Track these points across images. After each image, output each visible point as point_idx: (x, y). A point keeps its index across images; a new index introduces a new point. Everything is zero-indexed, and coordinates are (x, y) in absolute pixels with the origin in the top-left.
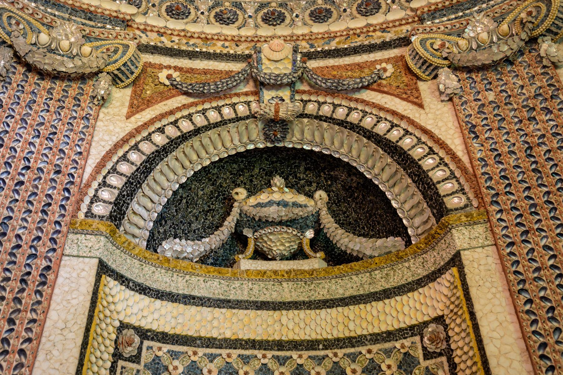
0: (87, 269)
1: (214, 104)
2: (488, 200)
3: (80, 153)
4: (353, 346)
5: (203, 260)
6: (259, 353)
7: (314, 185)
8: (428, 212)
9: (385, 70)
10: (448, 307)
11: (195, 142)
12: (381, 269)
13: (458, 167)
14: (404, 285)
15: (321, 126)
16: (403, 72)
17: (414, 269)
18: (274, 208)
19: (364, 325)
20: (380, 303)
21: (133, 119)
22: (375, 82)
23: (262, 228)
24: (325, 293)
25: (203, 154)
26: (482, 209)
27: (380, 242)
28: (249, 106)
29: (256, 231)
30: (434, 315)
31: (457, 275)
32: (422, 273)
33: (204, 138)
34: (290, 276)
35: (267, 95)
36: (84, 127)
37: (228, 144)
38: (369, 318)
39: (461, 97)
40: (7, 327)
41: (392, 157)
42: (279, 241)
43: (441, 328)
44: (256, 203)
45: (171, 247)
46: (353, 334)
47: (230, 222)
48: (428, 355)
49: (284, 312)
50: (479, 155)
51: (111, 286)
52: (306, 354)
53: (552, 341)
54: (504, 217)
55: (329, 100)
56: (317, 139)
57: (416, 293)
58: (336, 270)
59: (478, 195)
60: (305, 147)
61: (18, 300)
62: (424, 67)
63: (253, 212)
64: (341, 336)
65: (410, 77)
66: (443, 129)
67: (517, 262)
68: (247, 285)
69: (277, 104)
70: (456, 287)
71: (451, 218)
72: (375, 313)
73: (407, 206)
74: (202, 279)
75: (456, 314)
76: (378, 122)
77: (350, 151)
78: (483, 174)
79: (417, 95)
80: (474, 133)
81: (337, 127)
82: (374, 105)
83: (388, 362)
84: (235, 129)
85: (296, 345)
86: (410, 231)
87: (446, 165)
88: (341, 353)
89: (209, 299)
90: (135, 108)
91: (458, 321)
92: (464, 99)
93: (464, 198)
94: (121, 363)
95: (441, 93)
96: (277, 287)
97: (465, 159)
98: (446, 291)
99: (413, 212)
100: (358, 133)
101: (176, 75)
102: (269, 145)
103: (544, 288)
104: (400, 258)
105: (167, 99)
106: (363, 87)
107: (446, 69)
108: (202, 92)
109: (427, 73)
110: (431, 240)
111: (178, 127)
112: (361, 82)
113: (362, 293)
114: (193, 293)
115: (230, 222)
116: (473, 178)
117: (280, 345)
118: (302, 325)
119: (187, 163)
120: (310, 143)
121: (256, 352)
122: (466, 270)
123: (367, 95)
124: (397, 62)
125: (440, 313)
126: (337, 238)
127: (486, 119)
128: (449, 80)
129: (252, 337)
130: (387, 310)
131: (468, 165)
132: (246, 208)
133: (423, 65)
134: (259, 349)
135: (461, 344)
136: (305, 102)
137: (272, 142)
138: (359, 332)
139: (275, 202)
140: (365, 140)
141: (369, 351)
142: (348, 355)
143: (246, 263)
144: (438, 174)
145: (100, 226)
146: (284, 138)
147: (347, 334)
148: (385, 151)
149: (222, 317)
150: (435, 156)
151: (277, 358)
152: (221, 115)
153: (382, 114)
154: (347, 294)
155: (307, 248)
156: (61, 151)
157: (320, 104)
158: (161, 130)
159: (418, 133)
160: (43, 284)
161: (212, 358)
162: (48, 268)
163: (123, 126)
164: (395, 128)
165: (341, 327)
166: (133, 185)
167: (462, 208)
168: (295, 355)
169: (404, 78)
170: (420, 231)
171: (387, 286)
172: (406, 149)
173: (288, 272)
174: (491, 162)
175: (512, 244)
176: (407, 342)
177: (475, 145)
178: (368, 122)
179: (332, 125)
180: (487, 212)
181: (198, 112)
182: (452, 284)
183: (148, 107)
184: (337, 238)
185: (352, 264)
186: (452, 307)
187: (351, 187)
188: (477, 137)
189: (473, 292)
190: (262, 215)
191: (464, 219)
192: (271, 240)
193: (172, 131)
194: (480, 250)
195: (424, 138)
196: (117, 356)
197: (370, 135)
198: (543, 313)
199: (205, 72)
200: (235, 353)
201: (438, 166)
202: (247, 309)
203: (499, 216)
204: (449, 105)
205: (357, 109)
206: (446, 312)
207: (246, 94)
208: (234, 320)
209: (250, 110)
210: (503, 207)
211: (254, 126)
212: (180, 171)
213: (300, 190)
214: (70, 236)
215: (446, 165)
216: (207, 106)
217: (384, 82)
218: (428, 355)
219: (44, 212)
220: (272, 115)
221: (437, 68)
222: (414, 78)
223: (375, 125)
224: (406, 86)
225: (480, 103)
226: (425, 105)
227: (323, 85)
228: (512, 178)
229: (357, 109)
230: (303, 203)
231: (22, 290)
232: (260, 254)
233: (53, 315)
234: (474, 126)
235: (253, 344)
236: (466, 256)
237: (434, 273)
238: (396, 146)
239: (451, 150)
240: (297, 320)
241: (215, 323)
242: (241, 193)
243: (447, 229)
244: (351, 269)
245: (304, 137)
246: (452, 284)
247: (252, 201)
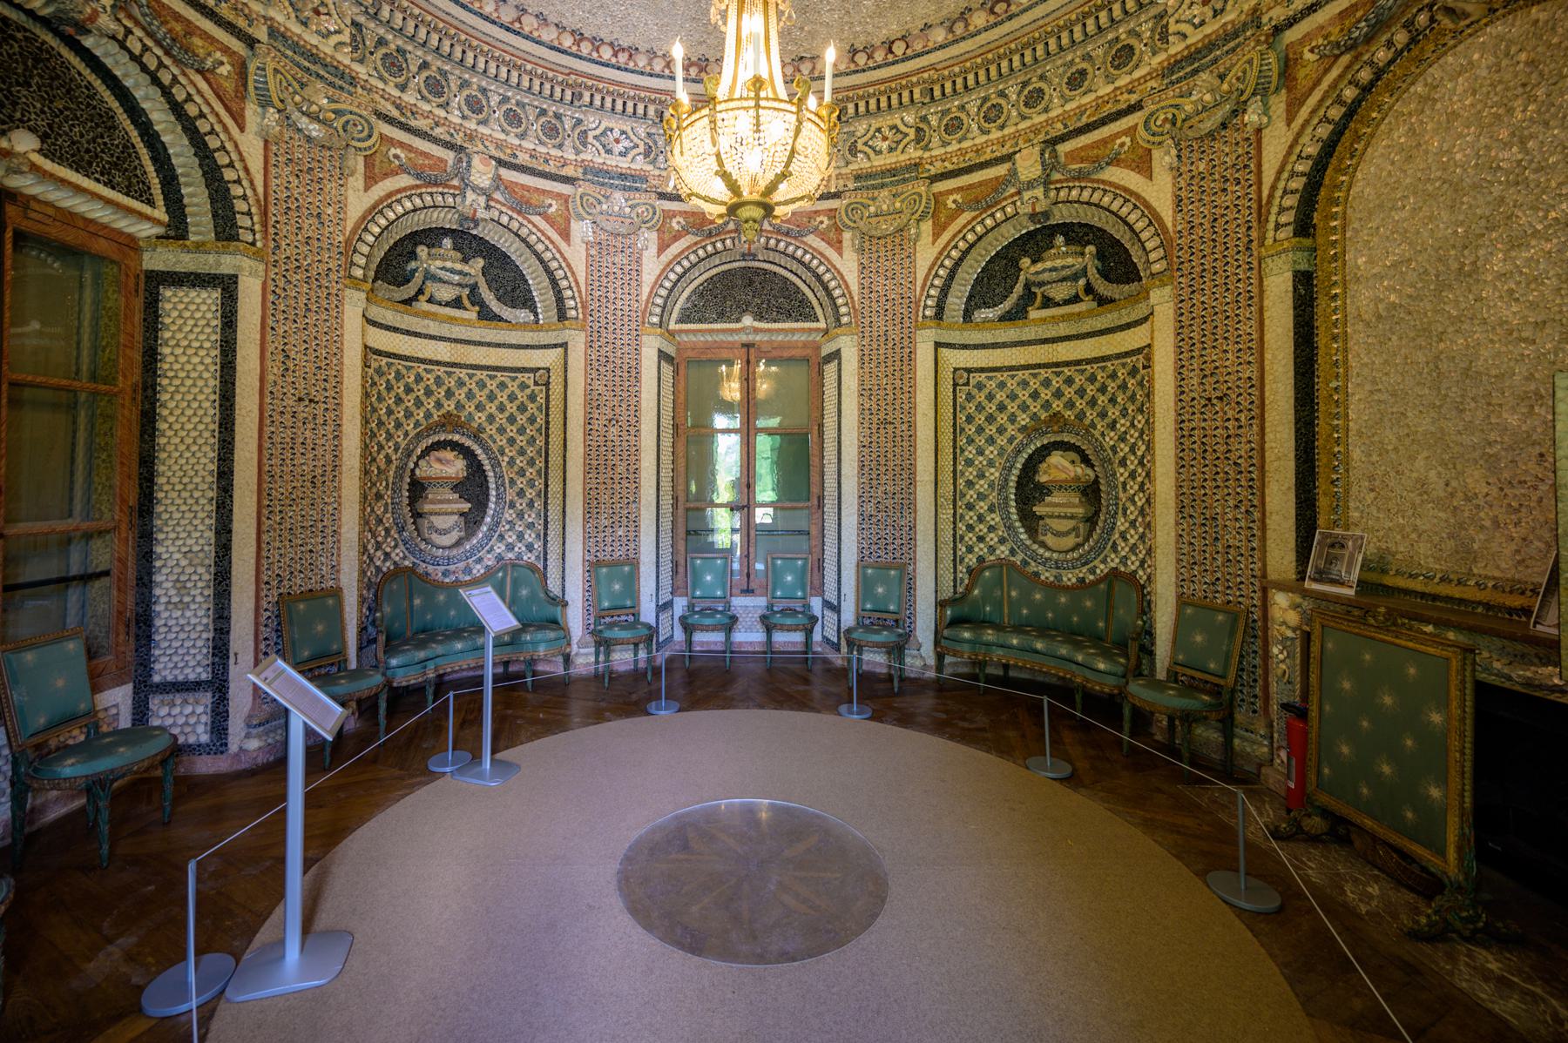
5: (1002, 319)
47: (1019, 289)
68: (1034, 329)
90: (936, 235)
101: (958, 197)
115: (1019, 289)
117: (1057, 365)
166: (945, 291)
199: (981, 184)
232: (1048, 302)
235: (1039, 366)
242: (1025, 262)
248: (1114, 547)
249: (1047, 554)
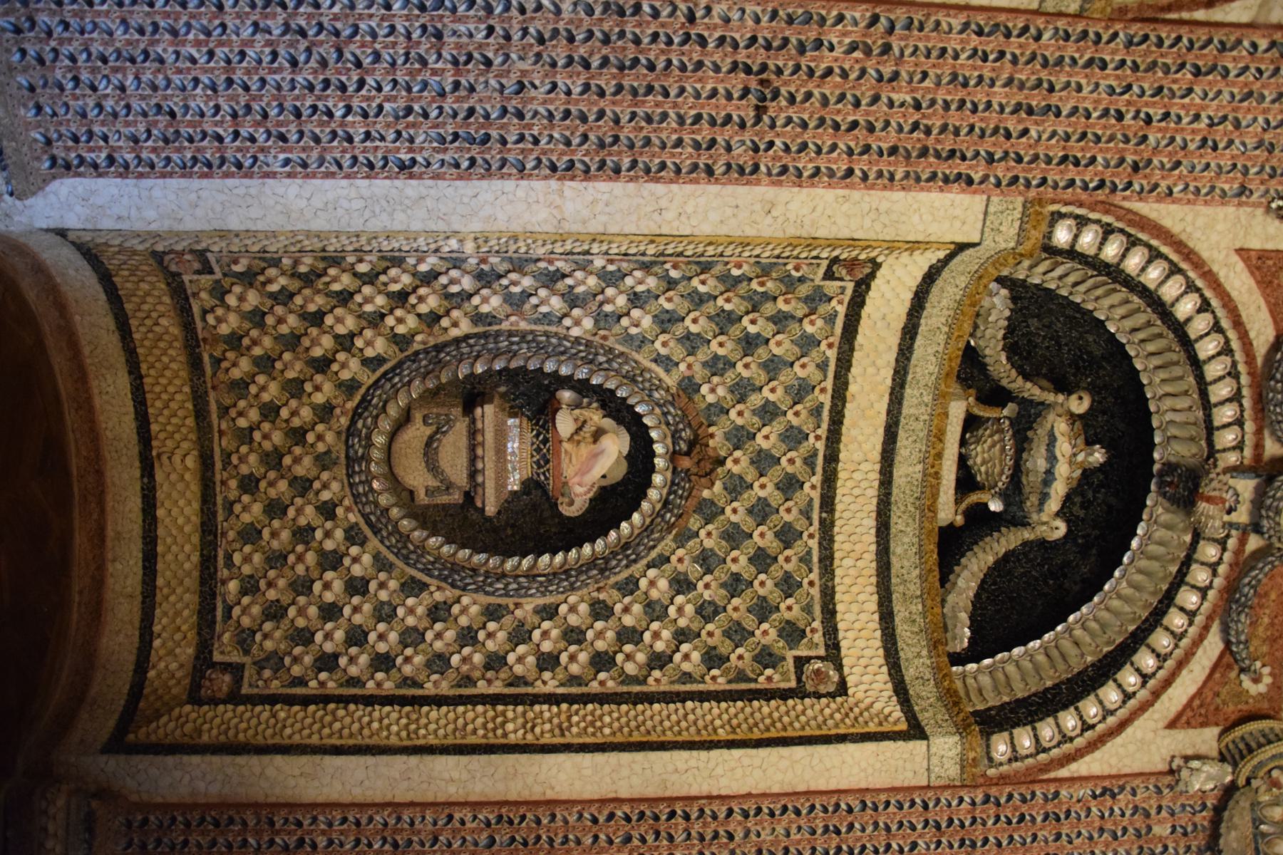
0: (966, 228)
1: (1245, 392)
2: (993, 791)
3: (1171, 193)
4: (820, 561)
6: (823, 431)
7: (1082, 513)
8: (993, 701)
9: (1256, 681)
10: (856, 705)
11: (1178, 355)
12: (924, 614)
13: (1052, 761)
14: (895, 643)
15: (1173, 560)
16: (1244, 707)
17: (917, 662)
18: (1042, 464)
19: (847, 581)
20: (874, 607)
21: (1236, 258)
22: (1236, 661)
23: (1014, 435)
24: (900, 527)
25: (1156, 361)
26: (981, 780)
27: (964, 616)
28: (1234, 448)
29: (1011, 424)
30: (851, 681)
31: (896, 728)
32: (909, 674)
33: (1183, 370)
34: (931, 477)
35: (1246, 487)
36: (1223, 190)
37: (1168, 403)
38: (855, 589)
39: (1171, 787)
40: (885, 146)
41: (1093, 665)
42: (990, 456)
43: (832, 689)
44: (1057, 434)
45: (999, 304)
46: (836, 563)
48: (800, 662)
49: (878, 467)
50: (1064, 793)
52: (816, 495)
53: (802, 822)
54: (964, 805)
55: (1218, 582)
56: (1152, 548)
57: (882, 661)
58: (932, 547)
59: (1003, 780)
60: (1142, 524)
61: (924, 152)
62: (1242, 746)
63: (1042, 432)
64: (836, 546)
65: (1233, 717)
66: (1121, 750)
67: (901, 807)
69: (1223, 501)
70: (880, 724)
71: (977, 740)
72: (862, 597)
73: (1011, 669)
74: (941, 349)
75: (847, 715)
76: (1158, 656)
77: (1119, 597)
78: (1033, 794)
79: (1193, 722)
80: (1102, 794)
81: (1165, 587)
82: (1189, 655)
83: (796, 608)
84: (1192, 420)
85: (830, 480)
86: (972, 667)
87: (1058, 745)
88: (814, 544)
89: (908, 359)
91: (837, 716)
92: (1166, 791)
93: (1004, 759)
95: (1187, 759)
96: (916, 456)
97: (1064, 773)
98: (877, 706)
99: (1000, 676)
100: (1147, 619)
102: (1156, 467)
103: (863, 830)
104: (935, 645)
105: (1271, 312)
106: (1228, 644)
107: (1229, 778)
108: (1273, 378)
109: (1231, 746)
110: (951, 699)
111: (1207, 334)
112: (1239, 642)
113: (893, 581)
114: (919, 337)
116: (1030, 778)
118: (856, 492)
119: (1141, 335)
120: (1148, 536)
121: (825, 426)
122: (901, 743)
123: (1213, 646)
124: (1270, 700)
125: (850, 692)
126: (981, 555)
127: (1123, 815)
128: (1205, 779)
129: (846, 421)
130: (864, 617)
131: (1052, 775)
132: (1051, 417)
133: (1247, 745)
134: (829, 430)
135: (810, 713)
136: (1223, 544)
137: (1161, 474)
138: (838, 572)
139: (1053, 466)
140: (1131, 628)
141: (811, 584)
142: (809, 553)
143: (957, 411)
144: (1047, 730)
145: (1033, 241)
146: (1164, 495)
147: (837, 555)
148: (1105, 656)
149: (879, 378)
150: (1078, 731)
151: (815, 454)
152: (1222, 403)
153: (1170, 663)
154: (894, 560)
155: (974, 498)
156: (1178, 164)
157: (1213, 567)
158: (1205, 307)
159: (1122, 713)
160: (946, 180)
161: (822, 367)
162: (970, 181)
163: (1223, 245)
164: (1139, 680)
165: (847, 547)
167: (988, 753)
168: (817, 479)
169: (1231, 708)
170: (970, 681)
171: (897, 620)
172: (1101, 692)
173: (937, 475)
174: (1050, 807)
175: (926, 807)
176: (818, 637)
177: (1083, 792)
178: (1162, 640)
179: (1170, 579)
180: (975, 787)
181: (1234, 364)
182: (886, 717)
183: (1258, 282)
184: (981, 555)
185: (937, 573)
186: (856, 710)
187: (1065, 576)
188: (1094, 796)
189: (870, 747)
190: (1034, 445)
191: (972, 755)
192: (993, 446)
193: (1200, 324)
194: (925, 764)
195: (1111, 720)
197: (1138, 639)
198: (835, 821)
200: (826, 399)
201: (1060, 731)
202: (889, 412)
203: (967, 799)
204: (1163, 767)
205: (1190, 624)
206: (851, 700)
207: (1259, 446)
208: (873, 397)
209: (1224, 450)
210: (979, 809)
211: (1194, 450)
212: (1128, 324)
213: (1068, 498)
214: (1020, 199)
215: (1058, 745)
216: (1244, 380)
217: (1233, 674)
218: (800, 662)
219: (1065, 159)
220: (1206, 490)
221: (1235, 765)
222: (1228, 724)
223: (1153, 651)
224: (1217, 709)
225: (1153, 812)
226: (1173, 732)
227: (1246, 580)
228: (1019, 829)
229: (1190, 624)
230: (1046, 507)
231: (938, 155)
233: (898, 195)
234: (1113, 796)
236: (918, 746)
237: (906, 692)
238: (1108, 678)
239: (1082, 756)
240: (864, 484)
241: (871, 370)
243: (962, 729)
244: (930, 571)
245: (1157, 529)
246: (886, 717)
247: (1061, 427)
248: (413, 587)
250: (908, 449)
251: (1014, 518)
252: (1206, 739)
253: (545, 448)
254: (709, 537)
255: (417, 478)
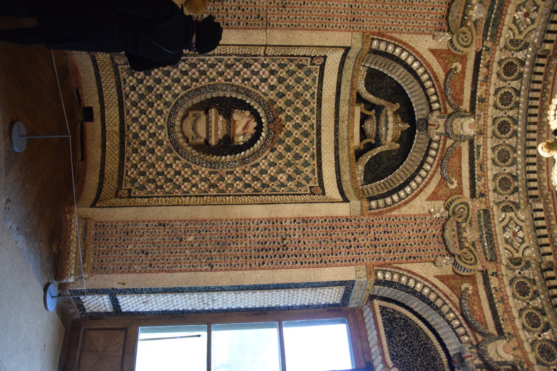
51: (342, 52)
94: (309, 59)
143: (358, 110)
196: (312, 58)
218: (311, 188)
220: (430, 122)
243: (360, 199)
249: (177, 123)
250: (343, 126)
251: (378, 143)
252: (440, 204)
253: (230, 123)
254: (281, 148)
255: (189, 131)
